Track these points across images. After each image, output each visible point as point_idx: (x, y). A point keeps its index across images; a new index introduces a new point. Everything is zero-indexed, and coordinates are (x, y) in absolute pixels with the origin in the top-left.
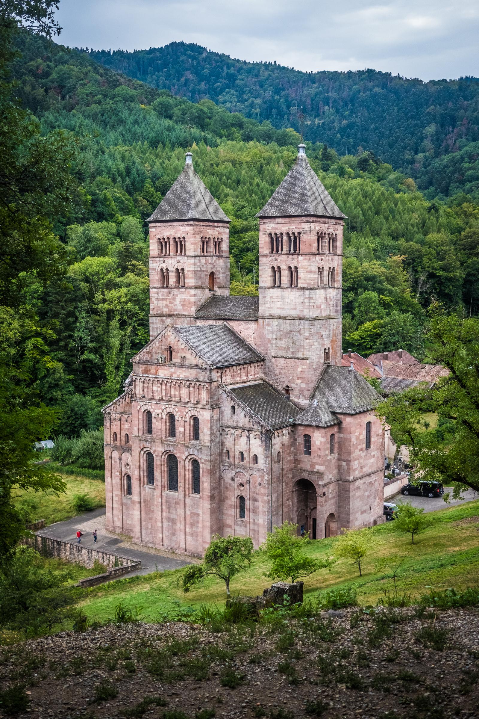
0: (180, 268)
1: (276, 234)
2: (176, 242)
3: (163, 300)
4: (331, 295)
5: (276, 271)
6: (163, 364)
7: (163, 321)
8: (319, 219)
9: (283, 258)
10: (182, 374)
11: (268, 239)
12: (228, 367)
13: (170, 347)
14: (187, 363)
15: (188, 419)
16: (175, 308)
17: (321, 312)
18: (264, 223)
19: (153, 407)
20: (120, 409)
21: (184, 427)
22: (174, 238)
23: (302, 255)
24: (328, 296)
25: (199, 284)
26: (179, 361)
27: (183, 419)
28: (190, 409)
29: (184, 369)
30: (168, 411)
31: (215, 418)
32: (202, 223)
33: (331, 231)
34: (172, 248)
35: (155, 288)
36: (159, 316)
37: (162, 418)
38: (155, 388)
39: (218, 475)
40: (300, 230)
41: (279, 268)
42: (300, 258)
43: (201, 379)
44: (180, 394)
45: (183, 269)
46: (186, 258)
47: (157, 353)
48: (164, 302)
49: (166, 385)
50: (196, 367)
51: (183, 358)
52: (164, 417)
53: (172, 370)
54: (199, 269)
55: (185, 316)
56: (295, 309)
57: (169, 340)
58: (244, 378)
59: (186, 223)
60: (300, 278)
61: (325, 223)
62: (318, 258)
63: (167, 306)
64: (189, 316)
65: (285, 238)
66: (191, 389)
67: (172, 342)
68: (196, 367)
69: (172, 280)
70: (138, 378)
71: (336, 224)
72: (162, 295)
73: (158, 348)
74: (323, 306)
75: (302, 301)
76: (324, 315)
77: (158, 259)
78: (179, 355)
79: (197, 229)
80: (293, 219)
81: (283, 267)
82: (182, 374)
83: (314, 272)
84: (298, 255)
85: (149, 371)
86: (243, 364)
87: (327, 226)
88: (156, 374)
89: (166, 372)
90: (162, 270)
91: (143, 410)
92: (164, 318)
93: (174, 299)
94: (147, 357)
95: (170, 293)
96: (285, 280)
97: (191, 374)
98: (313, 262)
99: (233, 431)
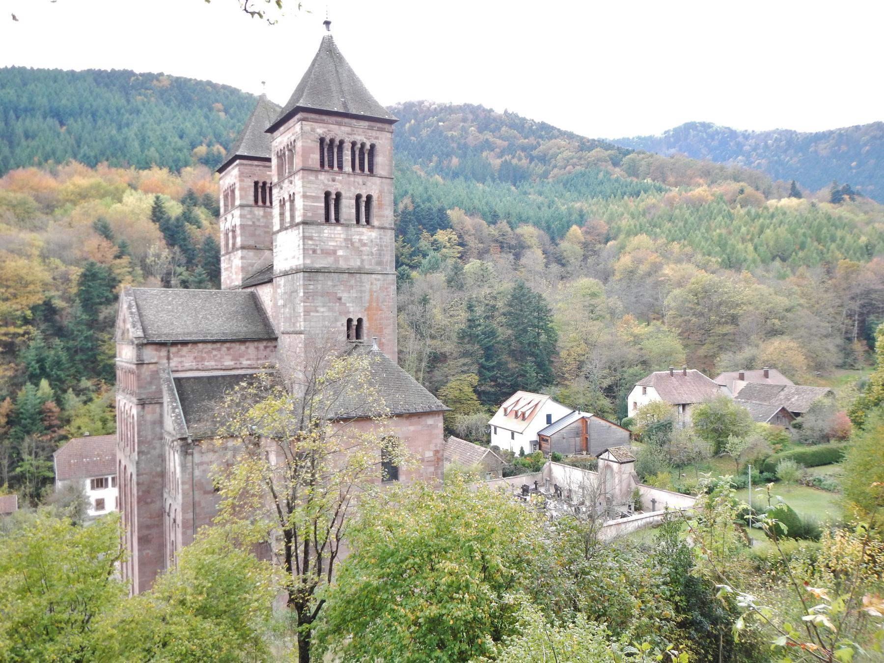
4: (364, 238)
8: (324, 117)
12: (184, 343)
17: (337, 260)
24: (356, 238)
25: (251, 242)
31: (149, 417)
32: (256, 163)
33: (359, 138)
39: (158, 505)
54: (250, 223)
58: (229, 363)
61: (340, 124)
62: (323, 177)
71: (371, 128)
74: (340, 253)
76: (343, 265)
79: (247, 170)
83: (315, 198)
86: (225, 342)
87: (348, 129)
98: (310, 182)
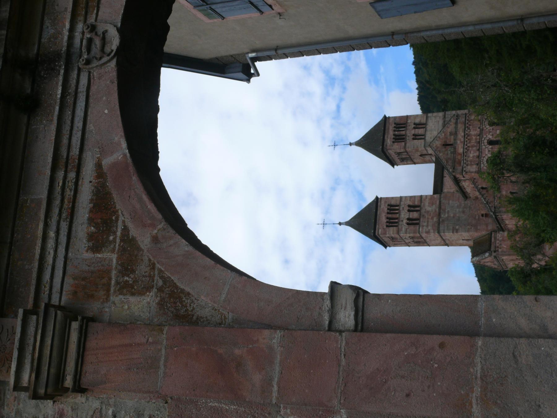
0: (407, 208)
1: (394, 139)
2: (390, 210)
3: (428, 222)
5: (416, 137)
6: (455, 148)
7: (443, 221)
9: (408, 132)
10: (461, 134)
11: (396, 144)
13: (444, 145)
14: (454, 130)
15: (491, 128)
16: (434, 211)
18: (386, 146)
20: (491, 199)
22: (388, 213)
23: (407, 120)
26: (452, 137)
30: (486, 144)
34: (394, 216)
35: (419, 228)
36: (439, 224)
37: (492, 148)
38: (471, 155)
41: (414, 135)
42: (409, 121)
43: (464, 119)
45: (409, 206)
46: (402, 203)
47: (447, 155)
48: (430, 220)
49: (469, 147)
51: (451, 134)
52: (490, 147)
53: (459, 142)
55: (440, 202)
56: (439, 122)
57: (438, 146)
59: (379, 204)
63: (432, 218)
64: (440, 198)
65: (396, 132)
68: (456, 123)
69: (415, 215)
70: (464, 169)
78: (449, 137)
80: (387, 128)
81: (413, 132)
82: (461, 134)
84: (407, 122)
88: (461, 154)
89: (460, 146)
90: (408, 224)
92: (441, 220)
93: (428, 212)
94: (450, 162)
95: (423, 216)
96: (421, 131)
97: (461, 127)
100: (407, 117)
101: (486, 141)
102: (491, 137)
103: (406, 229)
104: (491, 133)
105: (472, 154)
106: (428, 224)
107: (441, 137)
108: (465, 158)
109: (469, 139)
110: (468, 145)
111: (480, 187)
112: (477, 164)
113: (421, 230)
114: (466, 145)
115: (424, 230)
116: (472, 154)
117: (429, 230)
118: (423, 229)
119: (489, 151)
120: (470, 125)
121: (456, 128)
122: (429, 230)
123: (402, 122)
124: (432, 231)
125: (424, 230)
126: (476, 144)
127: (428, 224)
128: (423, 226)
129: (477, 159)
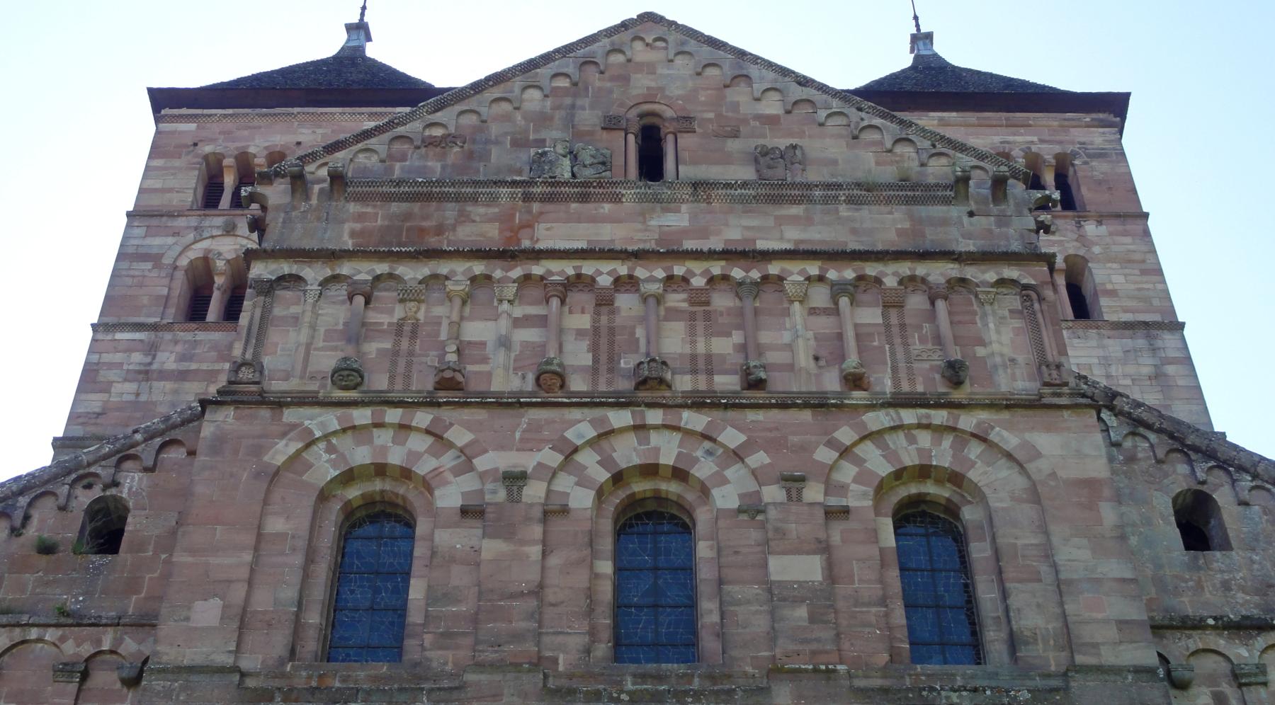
3: (182, 376)
15: (859, 498)
19: (460, 436)
21: (824, 548)
27: (814, 492)
28: (878, 419)
29: (796, 210)
30: (627, 452)
37: (554, 511)
40: (1069, 148)
42: (1090, 228)
44: (743, 348)
49: (604, 302)
50: (910, 191)
52: (582, 499)
53: (677, 220)
60: (1113, 293)
66: (871, 315)
67: (675, 90)
68: (910, 191)
70: (313, 273)
72: (183, 358)
73: (542, 119)
75: (1146, 370)
77: (181, 222)
78: (733, 145)
85: (440, 230)
91: (324, 468)
99: (1242, 652)
100: (1133, 217)
101: (668, 450)
102: (726, 498)
103: (156, 259)
104: (773, 493)
105: (498, 340)
106: (163, 375)
107: (739, 95)
108: (460, 270)
109: (699, 299)
110: (626, 303)
111: (132, 482)
112: (349, 375)
113: (119, 336)
114: (626, 283)
115: (118, 357)
116: (498, 340)
117: (108, 391)
118: (130, 348)
119: (514, 479)
120: (892, 304)
121: (865, 192)
122: (106, 388)
123: (1085, 193)
124: (95, 402)
125: (118, 357)
126: (628, 362)
127: (163, 375)
128: (152, 349)
129: (423, 382)
